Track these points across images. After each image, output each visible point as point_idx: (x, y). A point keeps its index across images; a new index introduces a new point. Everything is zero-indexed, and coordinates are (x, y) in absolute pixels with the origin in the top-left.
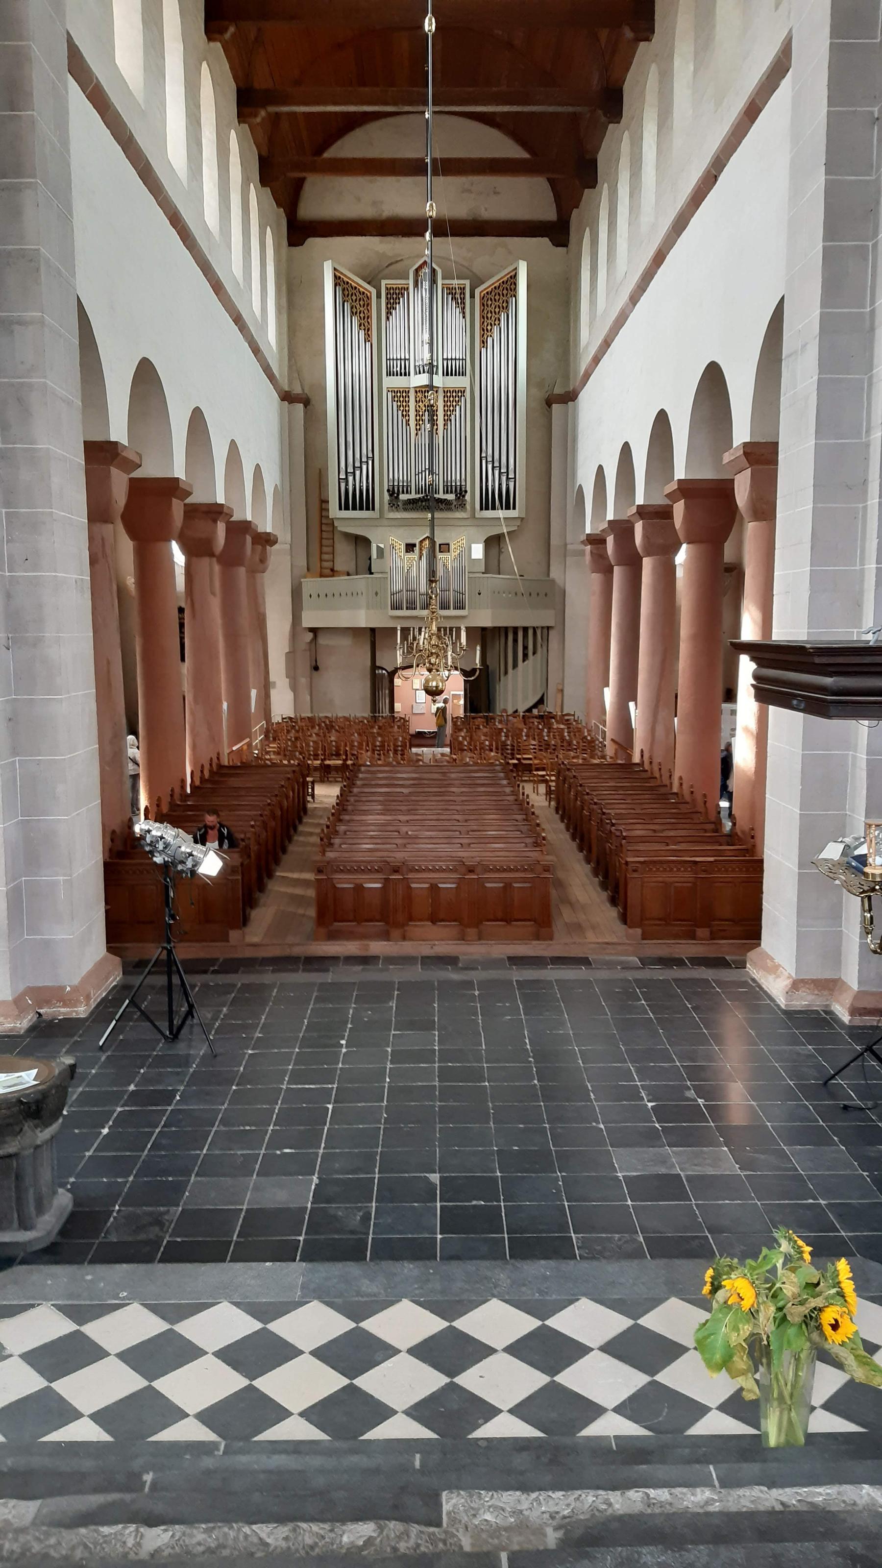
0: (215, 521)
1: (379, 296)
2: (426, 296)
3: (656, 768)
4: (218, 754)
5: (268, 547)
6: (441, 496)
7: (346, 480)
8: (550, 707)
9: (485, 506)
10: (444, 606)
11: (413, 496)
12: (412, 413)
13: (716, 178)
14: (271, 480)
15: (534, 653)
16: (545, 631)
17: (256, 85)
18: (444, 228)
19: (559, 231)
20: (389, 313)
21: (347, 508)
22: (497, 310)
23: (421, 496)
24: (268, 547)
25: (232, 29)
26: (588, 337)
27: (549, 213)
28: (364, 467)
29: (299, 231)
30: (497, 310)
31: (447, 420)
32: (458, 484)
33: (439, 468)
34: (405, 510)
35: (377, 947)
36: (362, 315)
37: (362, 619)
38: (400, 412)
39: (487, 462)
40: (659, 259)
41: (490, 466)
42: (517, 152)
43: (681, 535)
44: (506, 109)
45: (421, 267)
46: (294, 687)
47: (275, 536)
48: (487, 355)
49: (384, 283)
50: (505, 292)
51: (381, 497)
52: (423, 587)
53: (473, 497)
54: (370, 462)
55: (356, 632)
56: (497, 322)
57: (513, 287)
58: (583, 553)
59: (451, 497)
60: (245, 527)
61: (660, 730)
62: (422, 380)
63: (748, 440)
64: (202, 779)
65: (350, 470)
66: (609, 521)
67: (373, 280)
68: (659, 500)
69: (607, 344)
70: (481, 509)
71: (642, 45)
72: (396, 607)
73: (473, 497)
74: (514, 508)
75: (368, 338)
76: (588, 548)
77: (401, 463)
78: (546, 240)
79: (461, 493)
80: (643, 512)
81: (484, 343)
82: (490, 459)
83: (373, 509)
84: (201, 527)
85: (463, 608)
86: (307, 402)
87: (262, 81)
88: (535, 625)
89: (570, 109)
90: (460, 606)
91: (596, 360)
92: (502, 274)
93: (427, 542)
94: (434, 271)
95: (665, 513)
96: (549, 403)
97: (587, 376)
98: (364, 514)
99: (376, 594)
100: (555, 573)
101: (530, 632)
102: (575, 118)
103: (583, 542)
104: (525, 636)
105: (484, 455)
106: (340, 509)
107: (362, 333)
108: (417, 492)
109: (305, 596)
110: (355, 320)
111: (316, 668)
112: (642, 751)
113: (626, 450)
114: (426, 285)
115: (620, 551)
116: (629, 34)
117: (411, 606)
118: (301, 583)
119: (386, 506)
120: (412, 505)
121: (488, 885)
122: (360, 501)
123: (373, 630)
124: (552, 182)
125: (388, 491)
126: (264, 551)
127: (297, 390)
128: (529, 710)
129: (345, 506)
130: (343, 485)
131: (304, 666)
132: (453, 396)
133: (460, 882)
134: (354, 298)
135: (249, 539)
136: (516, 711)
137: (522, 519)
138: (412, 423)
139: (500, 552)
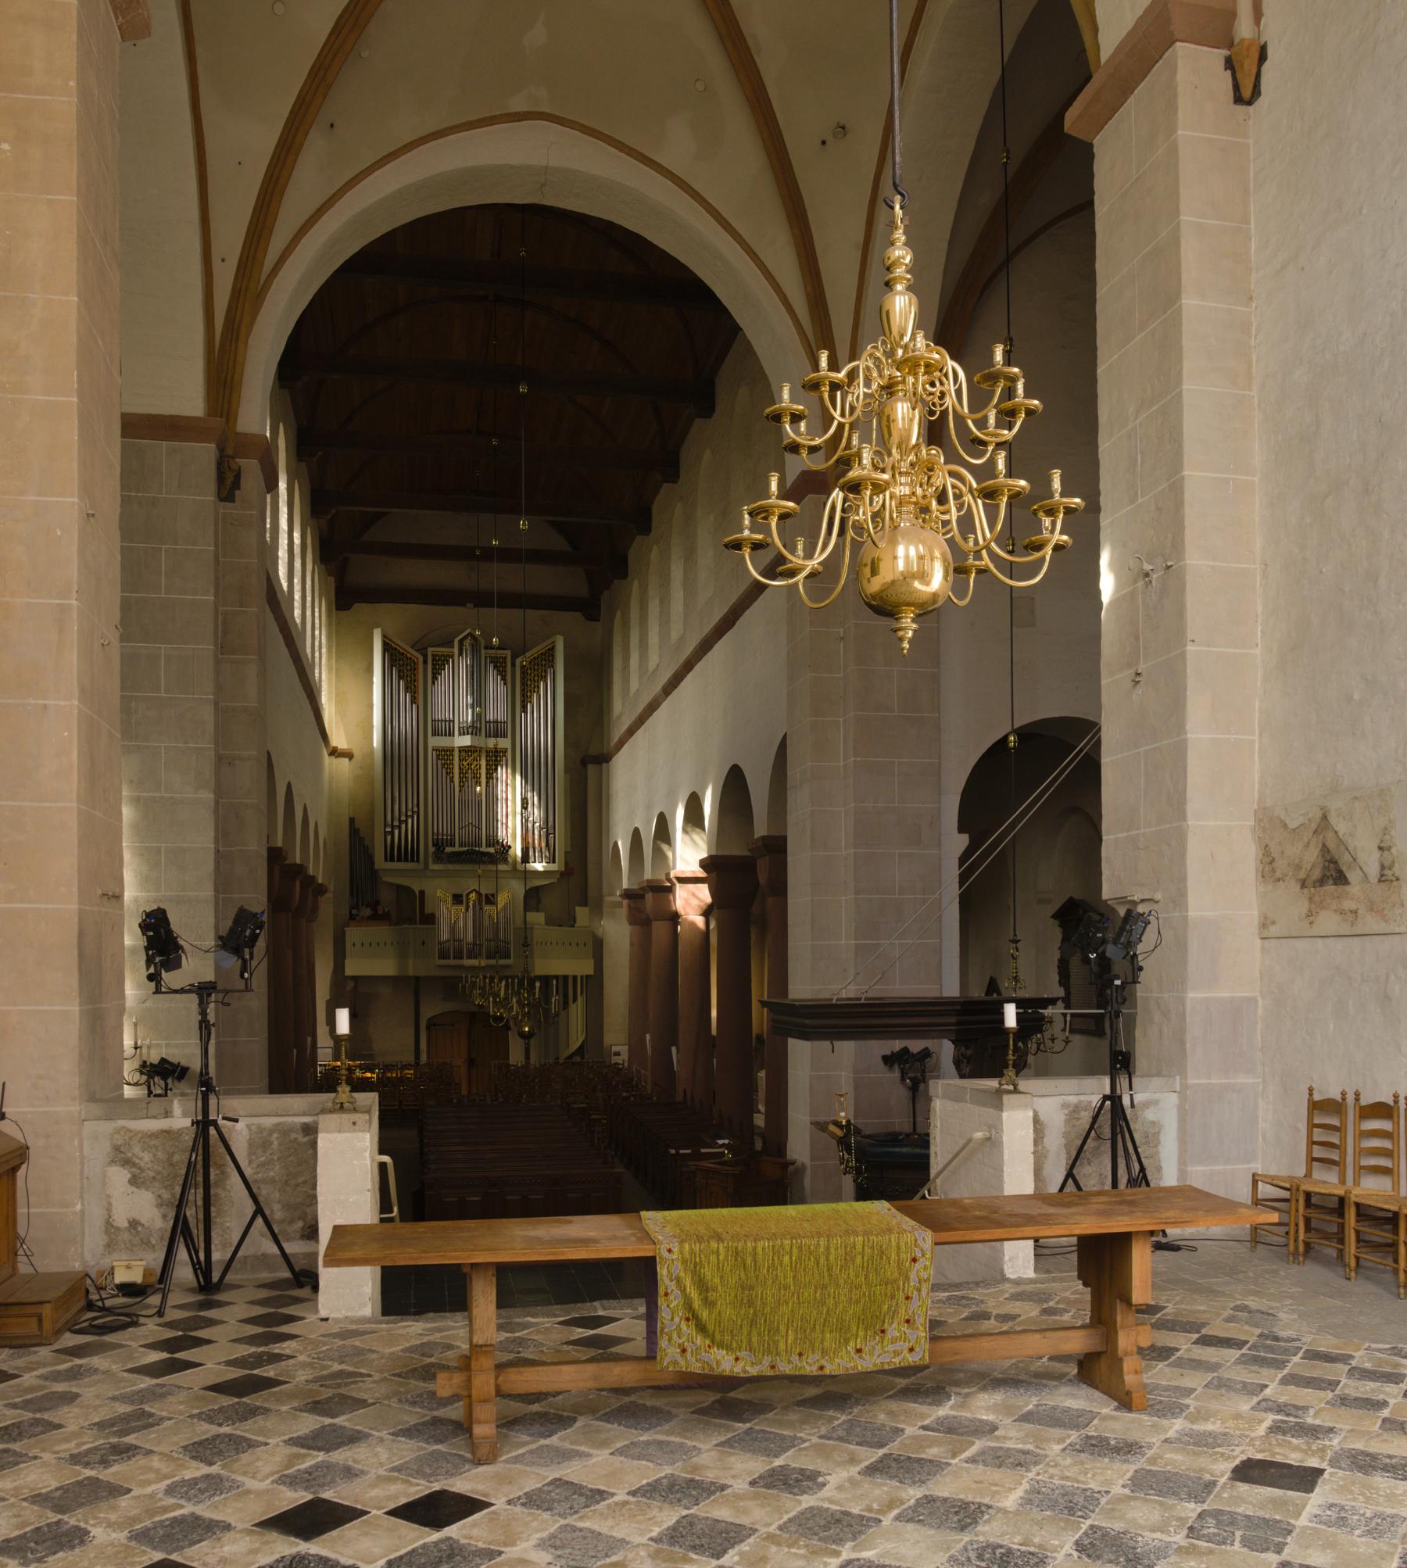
1: (425, 662)
6: (484, 849)
7: (392, 833)
11: (457, 849)
20: (435, 678)
21: (392, 860)
34: (450, 862)
45: (465, 638)
49: (430, 650)
51: (426, 847)
62: (466, 741)
67: (423, 651)
72: (444, 955)
75: (414, 700)
76: (625, 902)
78: (578, 614)
81: (524, 709)
92: (541, 648)
108: (461, 845)
109: (348, 945)
120: (456, 858)
122: (409, 854)
123: (417, 978)
129: (390, 857)
130: (389, 838)
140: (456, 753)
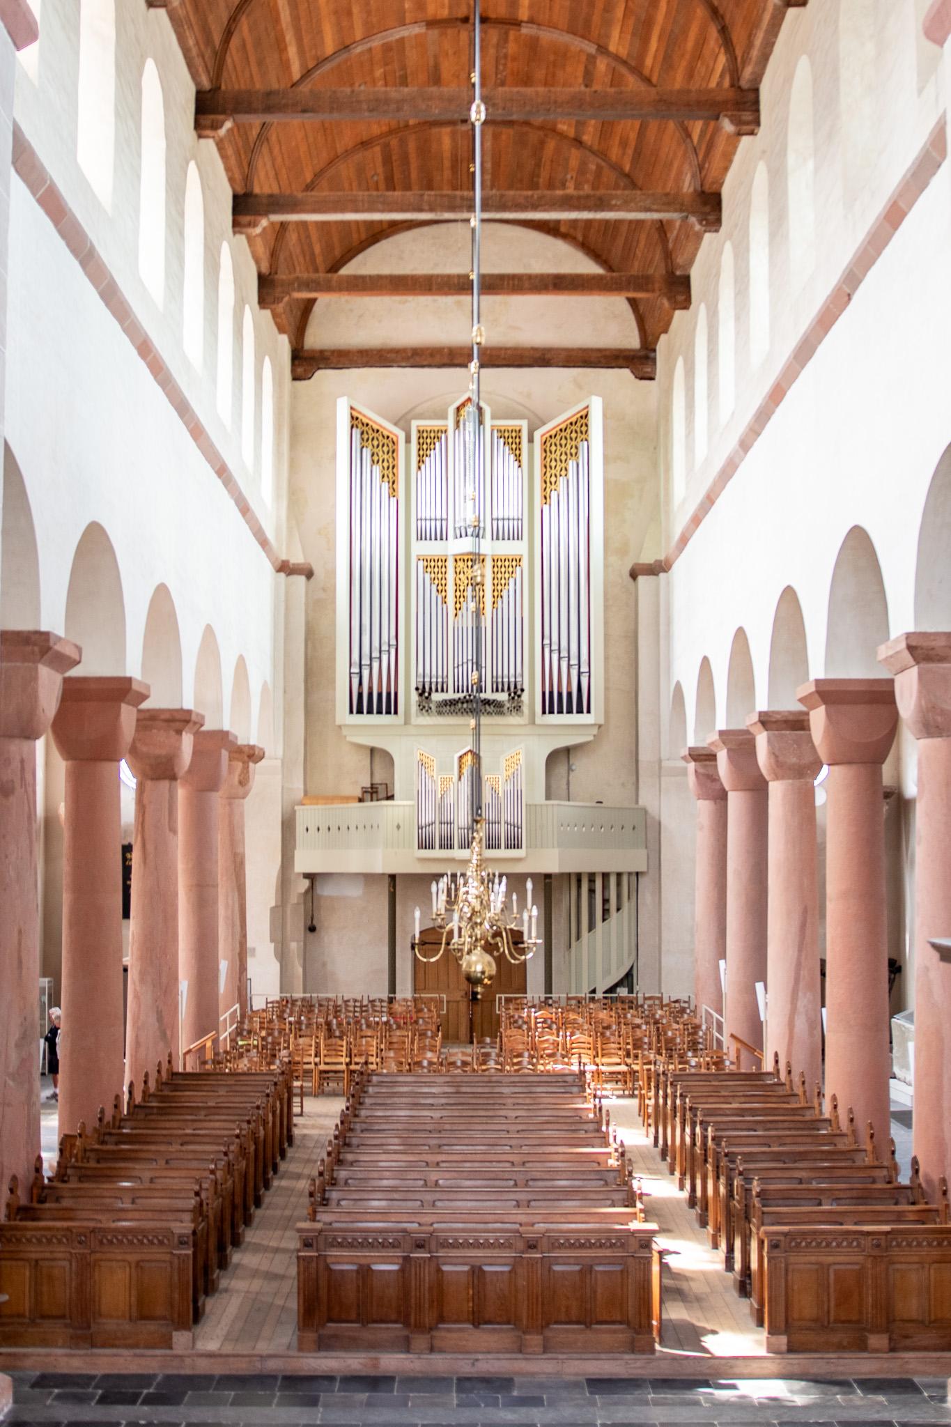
0: (179, 732)
1: (408, 440)
2: (470, 439)
3: (796, 1079)
4: (170, 1055)
5: (251, 765)
6: (488, 695)
8: (644, 988)
9: (548, 709)
10: (492, 844)
11: (451, 695)
12: (451, 588)
13: (849, 297)
14: (261, 672)
15: (618, 910)
16: (634, 878)
17: (257, 190)
18: (495, 358)
19: (640, 361)
21: (360, 711)
22: (563, 457)
23: (461, 695)
24: (251, 765)
25: (228, 124)
26: (683, 493)
27: (632, 341)
28: (385, 657)
29: (305, 362)
30: (563, 457)
31: (497, 596)
32: (512, 679)
33: (487, 661)
34: (440, 713)
35: (392, 1362)
36: (386, 464)
37: (382, 863)
38: (434, 587)
39: (551, 651)
40: (777, 394)
41: (555, 656)
42: (588, 267)
43: (823, 752)
44: (574, 215)
45: (463, 405)
46: (282, 956)
47: (261, 749)
48: (550, 512)
49: (415, 424)
50: (574, 435)
51: (408, 698)
52: (463, 817)
53: (532, 698)
54: (393, 651)
55: (369, 879)
56: (563, 472)
57: (584, 429)
58: (684, 772)
59: (503, 697)
60: (222, 737)
61: (801, 1024)
63: (911, 629)
64: (145, 1092)
65: (366, 661)
66: (721, 733)
68: (790, 705)
69: (709, 500)
70: (544, 712)
71: (745, 140)
72: (425, 844)
73: (532, 698)
74: (589, 712)
75: (393, 491)
76: (692, 766)
77: (431, 648)
78: (626, 373)
79: (516, 693)
80: (766, 721)
82: (555, 647)
83: (396, 712)
84: (160, 739)
85: (519, 846)
86: (309, 574)
87: (263, 185)
88: (620, 870)
89: (656, 216)
90: (514, 843)
91: (696, 520)
93: (469, 757)
94: (480, 409)
95: (798, 723)
96: (633, 575)
97: (684, 541)
98: (384, 719)
99: (398, 827)
100: (647, 798)
101: (613, 880)
102: (662, 227)
103: (684, 758)
104: (605, 887)
105: (547, 641)
106: (351, 712)
107: (385, 486)
109: (300, 829)
110: (377, 470)
111: (312, 929)
112: (776, 1055)
113: (740, 636)
114: (470, 426)
115: (735, 771)
116: (728, 126)
117: (447, 844)
118: (294, 812)
119: (414, 708)
120: (450, 706)
121: (557, 1268)
123: (393, 877)
124: (633, 303)
125: (417, 689)
126: (246, 770)
127: (297, 558)
128: (612, 990)
129: (358, 707)
131: (296, 925)
132: (506, 565)
133: (517, 1262)
134: (375, 443)
135: (225, 754)
136: (594, 991)
137: (600, 726)
138: (451, 600)
139: (570, 769)
140: (450, 564)
